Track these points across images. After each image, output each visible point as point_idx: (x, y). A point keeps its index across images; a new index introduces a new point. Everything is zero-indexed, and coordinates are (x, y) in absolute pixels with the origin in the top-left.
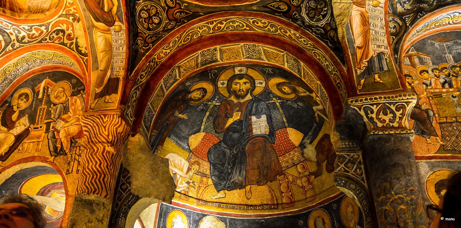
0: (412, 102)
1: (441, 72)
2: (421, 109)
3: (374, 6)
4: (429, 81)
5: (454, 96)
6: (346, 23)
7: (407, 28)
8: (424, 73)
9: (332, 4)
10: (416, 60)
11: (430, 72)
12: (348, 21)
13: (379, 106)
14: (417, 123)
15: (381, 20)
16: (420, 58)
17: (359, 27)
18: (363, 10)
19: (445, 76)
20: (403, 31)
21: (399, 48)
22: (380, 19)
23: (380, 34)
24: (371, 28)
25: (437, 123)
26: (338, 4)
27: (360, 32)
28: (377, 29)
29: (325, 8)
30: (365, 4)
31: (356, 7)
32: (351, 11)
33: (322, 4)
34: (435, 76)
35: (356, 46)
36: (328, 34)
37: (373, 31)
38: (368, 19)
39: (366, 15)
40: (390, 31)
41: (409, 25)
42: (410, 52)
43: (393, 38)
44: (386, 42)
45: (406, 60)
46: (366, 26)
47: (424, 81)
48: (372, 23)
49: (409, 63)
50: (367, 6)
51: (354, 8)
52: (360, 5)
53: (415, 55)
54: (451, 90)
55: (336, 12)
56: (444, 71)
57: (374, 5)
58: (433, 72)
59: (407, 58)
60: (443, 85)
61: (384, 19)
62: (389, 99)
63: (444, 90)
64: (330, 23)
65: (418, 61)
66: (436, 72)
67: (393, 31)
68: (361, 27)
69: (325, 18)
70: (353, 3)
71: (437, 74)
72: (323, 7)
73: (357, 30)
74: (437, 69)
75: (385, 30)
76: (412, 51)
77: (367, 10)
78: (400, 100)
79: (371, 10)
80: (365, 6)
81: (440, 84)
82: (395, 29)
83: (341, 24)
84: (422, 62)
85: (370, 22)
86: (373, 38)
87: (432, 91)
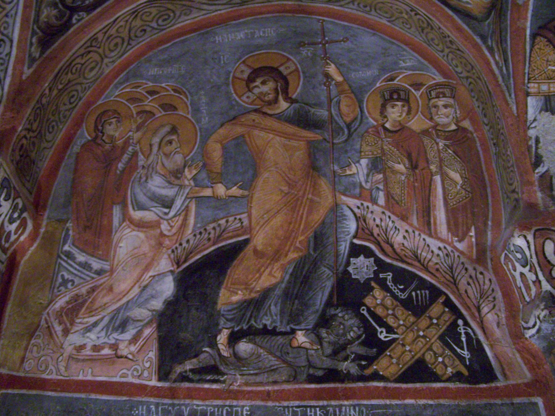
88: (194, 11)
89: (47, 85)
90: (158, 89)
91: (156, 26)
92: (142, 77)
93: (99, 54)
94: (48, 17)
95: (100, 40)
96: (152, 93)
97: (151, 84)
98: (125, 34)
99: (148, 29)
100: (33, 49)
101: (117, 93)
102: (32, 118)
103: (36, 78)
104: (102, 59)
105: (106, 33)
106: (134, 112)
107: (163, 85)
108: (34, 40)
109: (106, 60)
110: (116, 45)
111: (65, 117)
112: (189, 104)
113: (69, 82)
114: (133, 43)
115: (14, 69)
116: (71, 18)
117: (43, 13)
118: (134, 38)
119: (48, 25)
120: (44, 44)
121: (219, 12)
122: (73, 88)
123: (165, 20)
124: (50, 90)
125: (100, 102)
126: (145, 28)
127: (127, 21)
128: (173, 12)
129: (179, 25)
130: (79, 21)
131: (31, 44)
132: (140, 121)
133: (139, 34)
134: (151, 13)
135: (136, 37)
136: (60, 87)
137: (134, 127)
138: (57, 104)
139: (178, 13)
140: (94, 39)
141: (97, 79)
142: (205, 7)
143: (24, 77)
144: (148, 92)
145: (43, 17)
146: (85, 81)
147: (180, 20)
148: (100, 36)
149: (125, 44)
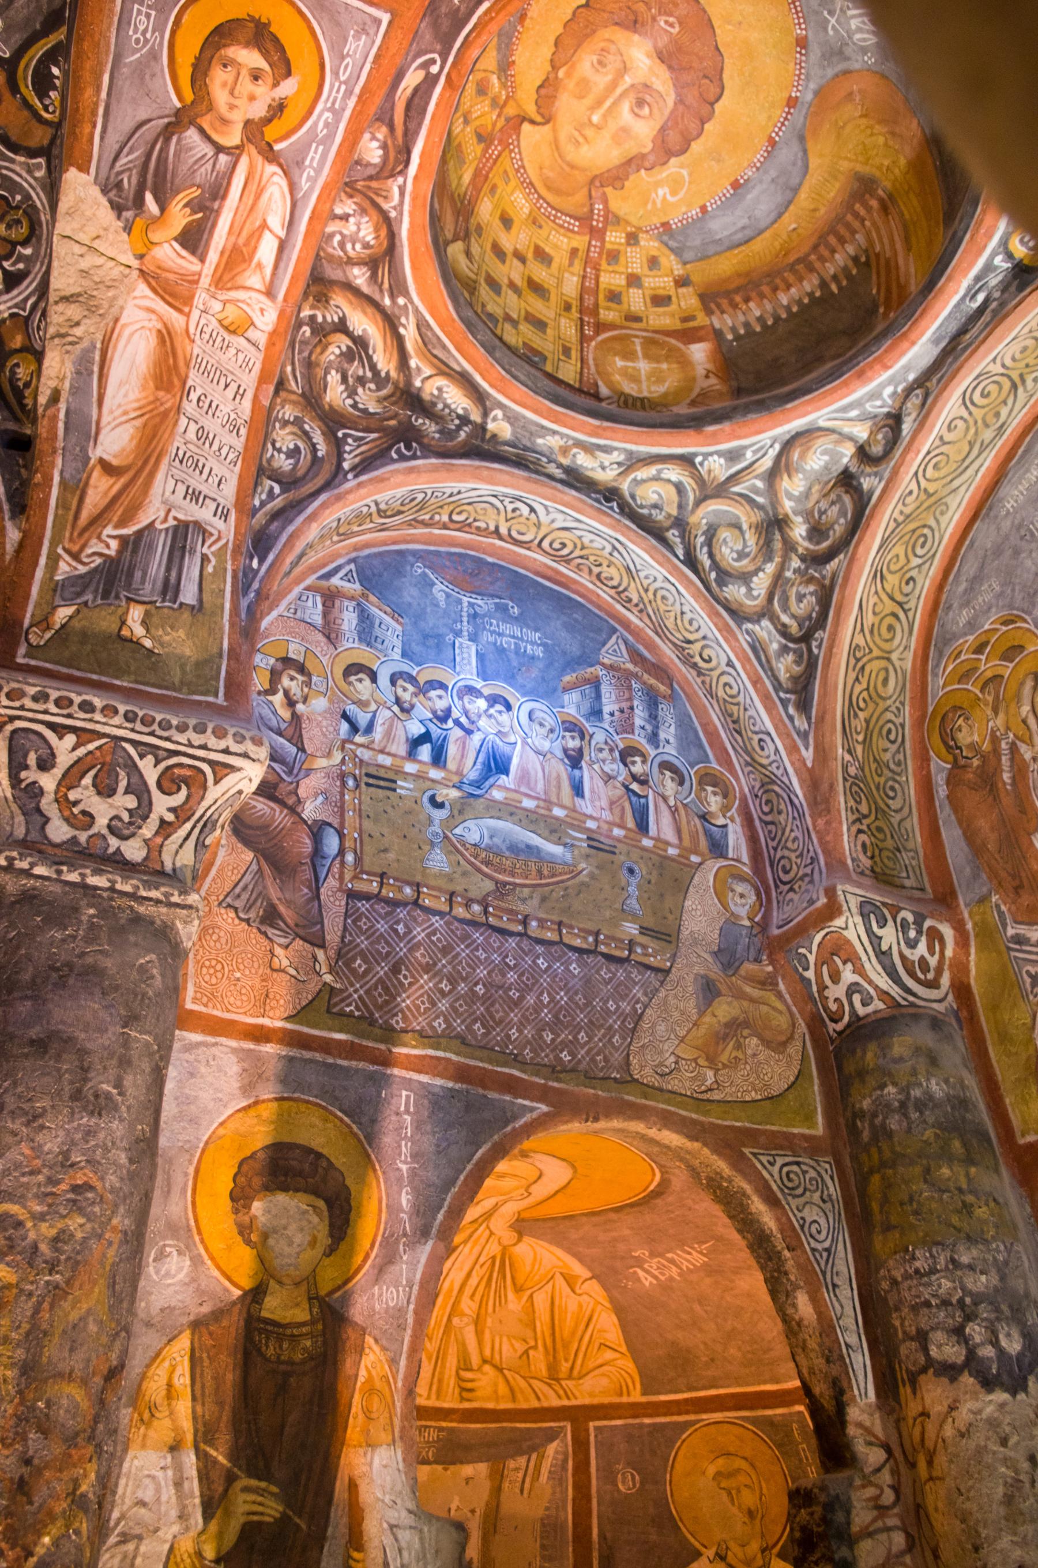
0: (239, 769)
1: (421, 696)
2: (299, 815)
3: (226, 328)
4: (369, 715)
5: (439, 799)
6: (85, 344)
8: (361, 676)
9: (55, 239)
10: (348, 619)
11: (384, 680)
12: (99, 337)
13: (91, 747)
14: (260, 870)
15: (240, 394)
16: (365, 618)
17: (135, 382)
18: (176, 319)
19: (430, 716)
20: (319, 481)
21: (277, 538)
22: (233, 387)
23: (215, 447)
24: (189, 407)
25: (340, 890)
26: (77, 249)
27: (136, 405)
28: (212, 425)
29: (25, 243)
30: (189, 300)
31: (148, 292)
32: (120, 302)
33: (18, 222)
35: (96, 454)
36: (9, 364)
37: (193, 428)
38: (188, 366)
39: (179, 341)
40: (269, 461)
41: (353, 469)
42: (336, 581)
43: (272, 489)
44: (228, 493)
45: (310, 603)
46: (168, 390)
47: (351, 709)
48: (199, 392)
49: (318, 620)
50: (195, 314)
51: (136, 293)
52: (171, 295)
53: (352, 598)
54: (435, 774)
55: (61, 282)
56: (433, 694)
57: (226, 323)
58: (393, 683)
59: (319, 599)
60: (416, 743)
61: (249, 395)
62: (129, 725)
63: (410, 768)
64: (27, 319)
65: (355, 622)
66: (405, 690)
67: (283, 463)
68: (144, 387)
69: (15, 292)
70: (141, 270)
71: (406, 696)
72: (21, 238)
73: (123, 391)
74: (412, 679)
75: (243, 439)
76: (348, 578)
77: (192, 330)
78: (190, 745)
79: (206, 337)
80: (187, 309)
81: (403, 739)
82: (291, 461)
83: (63, 336)
84: (366, 631)
85: (190, 383)
86: (181, 453)
88: (948, 500)
89: (840, 751)
90: (984, 639)
91: (919, 561)
92: (955, 637)
93: (878, 658)
94: (787, 670)
95: (862, 643)
96: (979, 649)
97: (971, 638)
98: (890, 606)
99: (914, 573)
100: (797, 723)
101: (941, 683)
102: (851, 803)
103: (823, 754)
104: (888, 659)
105: (862, 630)
106: (978, 692)
107: (987, 627)
108: (791, 710)
109: (894, 656)
110: (891, 628)
111: (899, 764)
112: (1032, 628)
113: (867, 722)
114: (912, 605)
115: (792, 764)
116: (810, 650)
117: (779, 669)
118: (905, 599)
119: (795, 679)
120: (804, 706)
121: (983, 469)
122: (881, 723)
123: (923, 546)
124: (849, 752)
125: (930, 709)
126: (908, 576)
127: (876, 593)
128: (924, 526)
129: (950, 530)
130: (819, 647)
131: (791, 718)
132: (990, 699)
133: (907, 589)
134: (897, 556)
135: (907, 595)
136: (860, 738)
137: (989, 712)
138: (875, 760)
139: (932, 523)
140: (854, 649)
141: (904, 685)
142: (956, 483)
143: (809, 764)
144: (975, 652)
145: (783, 676)
146: (889, 702)
147: (943, 526)
148: (859, 640)
149: (902, 615)
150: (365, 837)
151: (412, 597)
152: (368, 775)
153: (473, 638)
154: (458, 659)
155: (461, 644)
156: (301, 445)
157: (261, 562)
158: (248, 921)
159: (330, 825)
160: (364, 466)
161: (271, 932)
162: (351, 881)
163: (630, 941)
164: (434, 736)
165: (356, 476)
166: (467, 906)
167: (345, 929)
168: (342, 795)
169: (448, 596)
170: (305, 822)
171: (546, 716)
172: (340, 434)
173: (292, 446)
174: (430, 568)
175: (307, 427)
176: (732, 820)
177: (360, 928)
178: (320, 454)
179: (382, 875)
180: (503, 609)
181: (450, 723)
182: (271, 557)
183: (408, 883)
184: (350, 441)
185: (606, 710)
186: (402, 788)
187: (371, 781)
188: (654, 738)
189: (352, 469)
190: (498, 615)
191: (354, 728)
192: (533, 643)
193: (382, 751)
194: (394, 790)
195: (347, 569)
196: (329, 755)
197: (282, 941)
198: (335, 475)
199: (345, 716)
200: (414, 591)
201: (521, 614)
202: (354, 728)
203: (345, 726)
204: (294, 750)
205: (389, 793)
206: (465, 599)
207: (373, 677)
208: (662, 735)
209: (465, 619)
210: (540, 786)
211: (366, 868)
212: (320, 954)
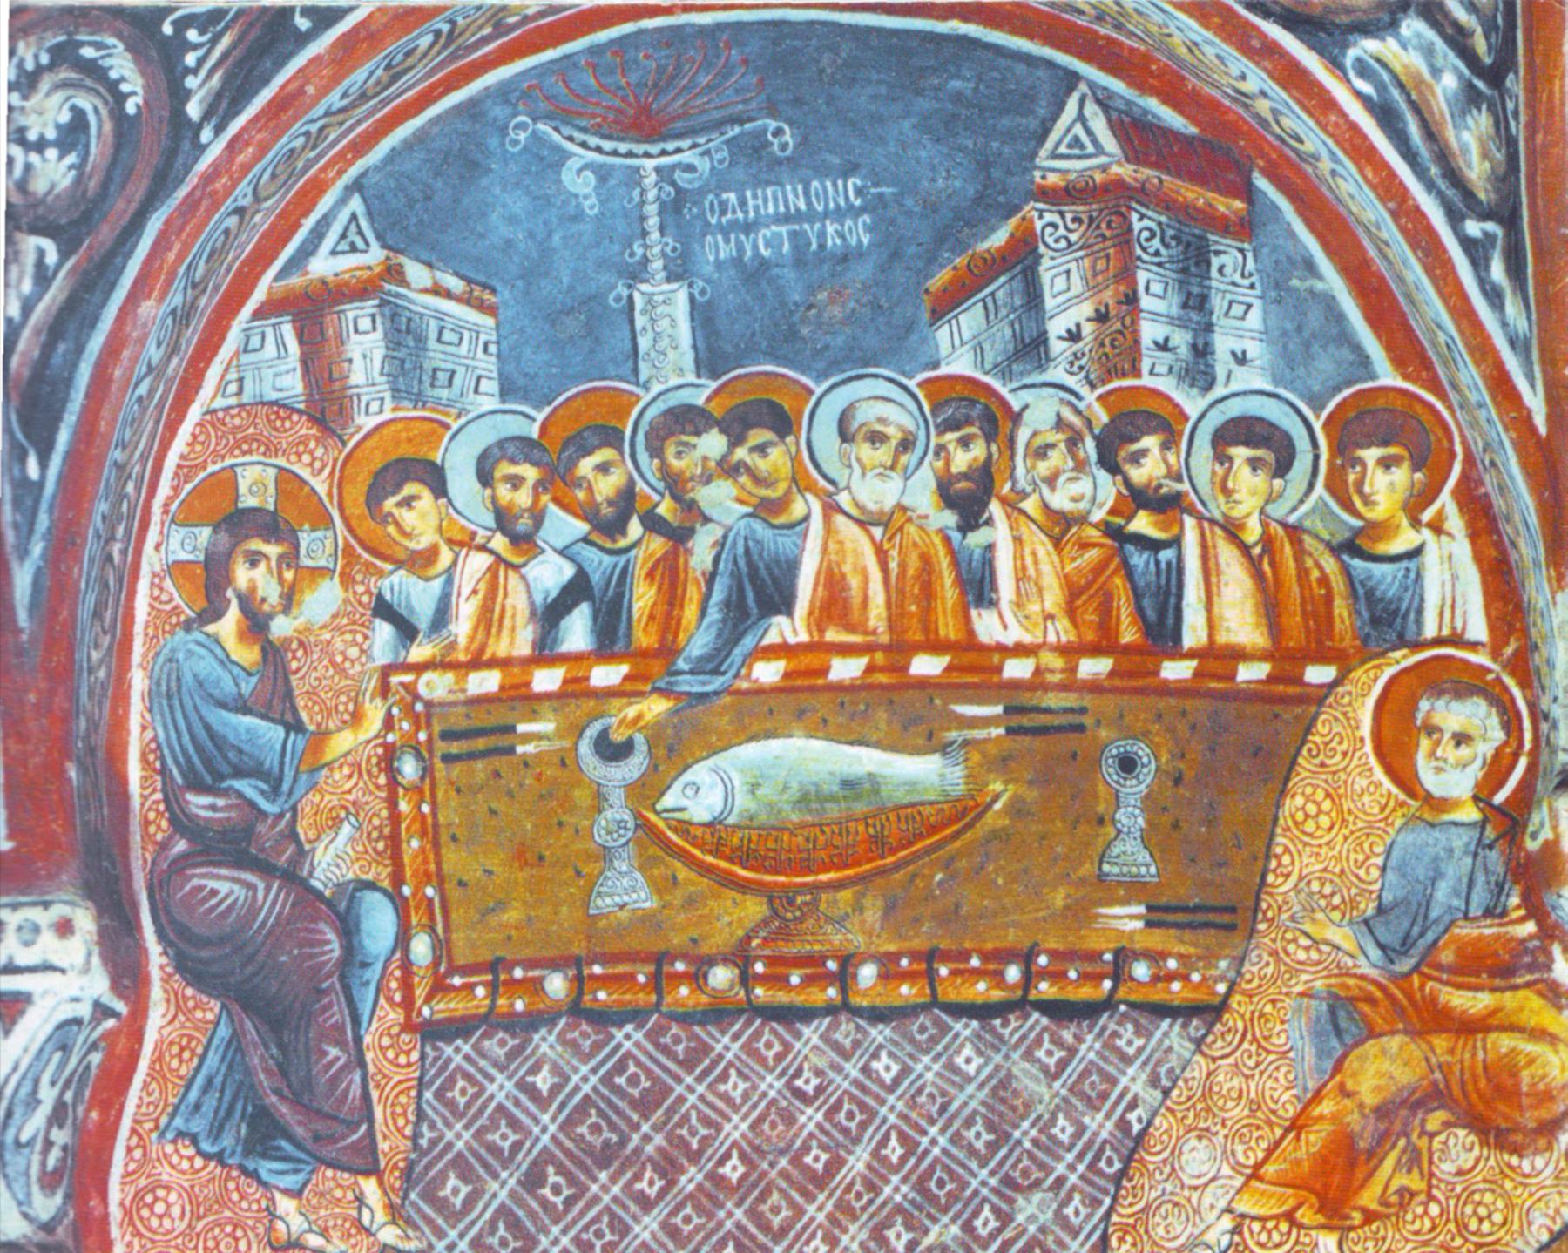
4: (437, 585)
5: (618, 737)
7: (186, 146)
8: (410, 489)
11: (463, 481)
20: (138, 190)
21: (68, 382)
34: (503, 519)
43: (41, 253)
45: (270, 350)
54: (605, 675)
58: (485, 477)
59: (288, 330)
60: (552, 614)
65: (378, 354)
66: (516, 482)
71: (523, 498)
82: (72, 158)
87: (436, 685)
150: (454, 893)
151: (512, 220)
152: (447, 736)
153: (678, 272)
154: (644, 343)
155: (649, 299)
156: (85, 102)
157: (44, 465)
158: (219, 1158)
159: (371, 886)
160: (224, 105)
161: (266, 1167)
162: (428, 1000)
163: (1118, 953)
164: (596, 578)
165: (219, 130)
166: (697, 978)
167: (421, 1115)
168: (392, 803)
169: (602, 174)
170: (319, 895)
171: (889, 411)
172: (167, 29)
173: (65, 117)
174: (548, 117)
175: (88, 52)
176: (1437, 527)
177: (451, 1104)
178: (130, 108)
179: (494, 966)
180: (753, 151)
181: (635, 528)
182: (63, 438)
183: (555, 964)
184: (192, 35)
185: (1056, 327)
186: (528, 738)
187: (455, 748)
188: (1199, 370)
189: (206, 116)
190: (739, 173)
191: (407, 631)
192: (839, 215)
193: (477, 662)
194: (510, 751)
195: (344, 216)
196: (357, 717)
197: (290, 1181)
198: (176, 138)
199: (384, 610)
200: (517, 203)
201: (804, 142)
202: (407, 631)
203: (384, 631)
204: (279, 732)
205: (499, 762)
206: (650, 164)
207: (436, 480)
208: (1223, 344)
209: (653, 222)
210: (877, 613)
211: (460, 961)
212: (369, 1186)
